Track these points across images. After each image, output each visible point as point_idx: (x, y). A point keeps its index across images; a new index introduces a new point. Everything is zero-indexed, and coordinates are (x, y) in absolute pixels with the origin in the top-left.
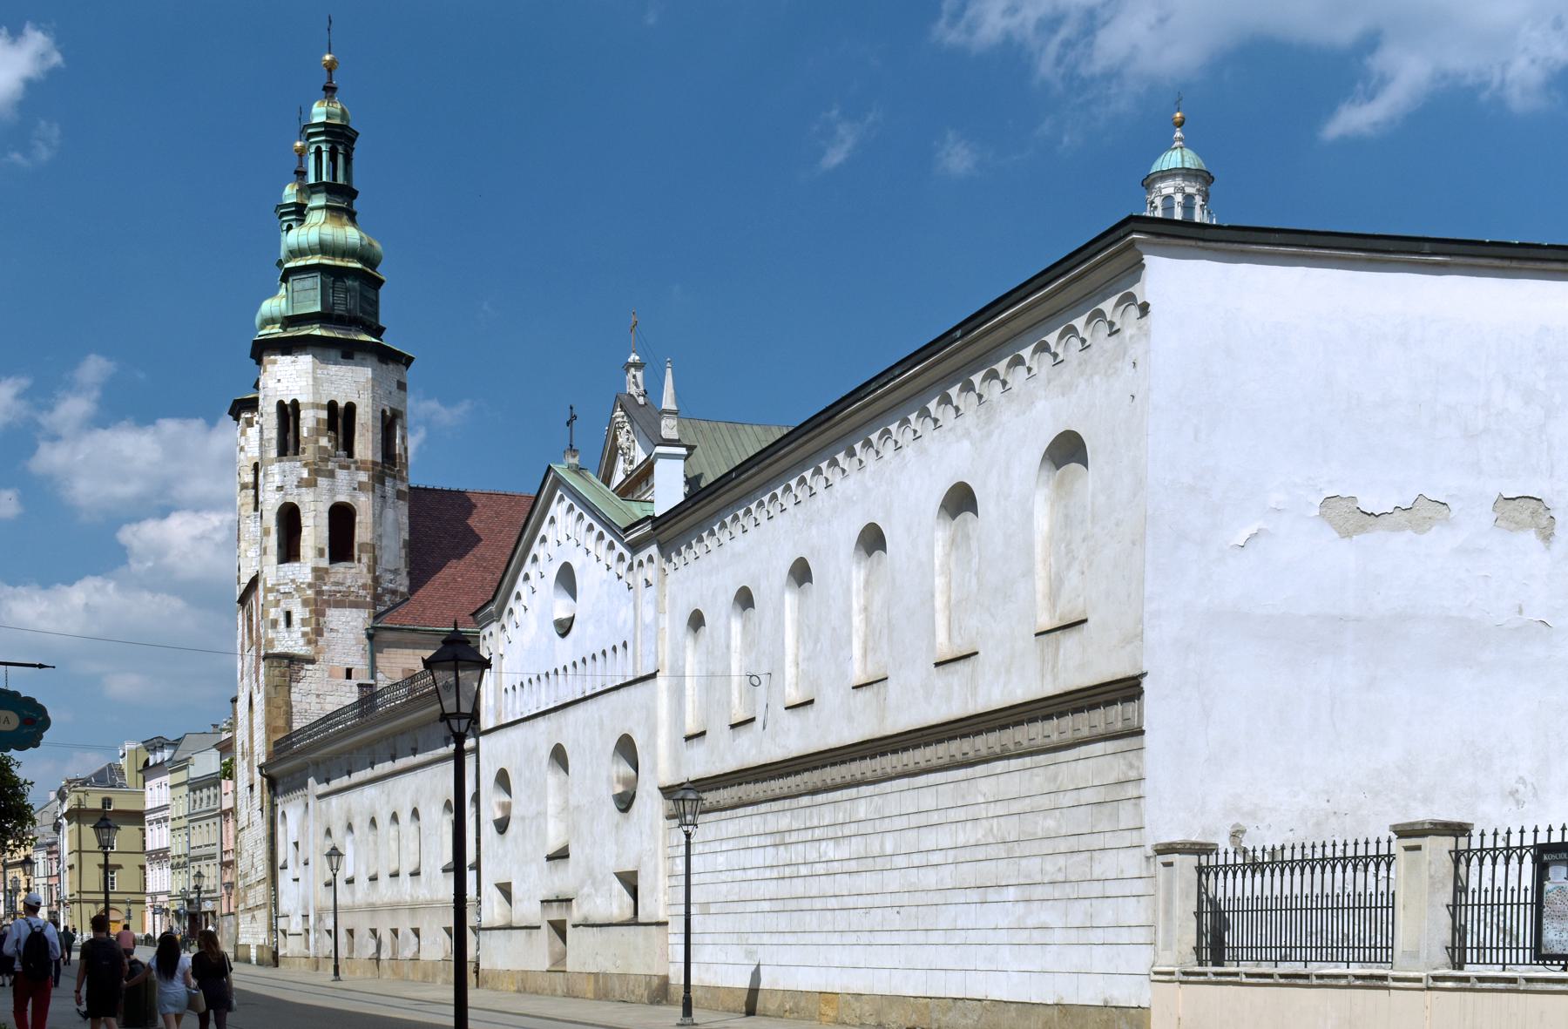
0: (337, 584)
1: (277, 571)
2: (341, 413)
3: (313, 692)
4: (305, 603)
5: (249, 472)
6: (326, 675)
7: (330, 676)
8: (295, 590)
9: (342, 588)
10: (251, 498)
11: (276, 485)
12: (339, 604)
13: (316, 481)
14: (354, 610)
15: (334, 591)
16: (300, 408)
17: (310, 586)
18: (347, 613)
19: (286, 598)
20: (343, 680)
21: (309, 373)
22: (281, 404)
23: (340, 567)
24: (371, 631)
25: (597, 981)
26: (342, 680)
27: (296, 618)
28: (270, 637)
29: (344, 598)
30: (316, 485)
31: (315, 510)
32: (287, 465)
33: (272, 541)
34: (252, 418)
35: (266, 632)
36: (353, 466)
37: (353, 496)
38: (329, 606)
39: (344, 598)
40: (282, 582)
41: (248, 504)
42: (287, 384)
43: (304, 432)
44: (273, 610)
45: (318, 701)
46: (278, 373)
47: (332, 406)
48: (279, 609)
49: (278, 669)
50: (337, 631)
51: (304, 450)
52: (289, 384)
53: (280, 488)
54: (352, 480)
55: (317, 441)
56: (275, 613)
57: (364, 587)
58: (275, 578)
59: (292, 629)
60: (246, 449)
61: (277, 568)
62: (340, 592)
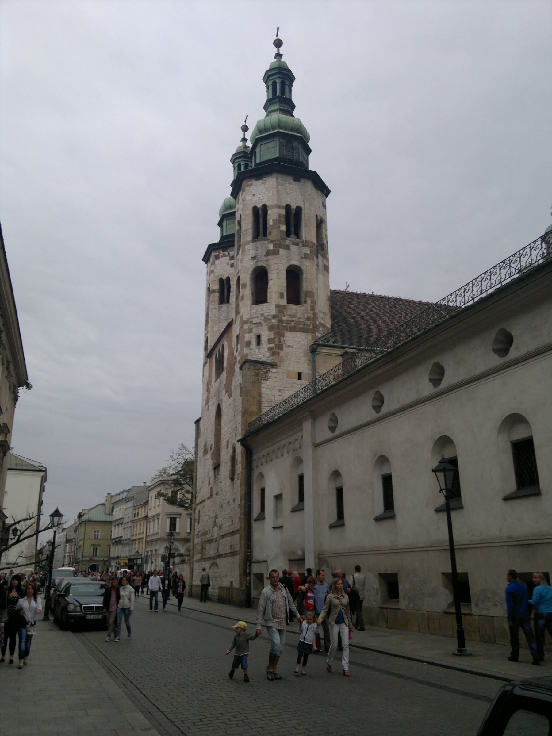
0: (291, 316)
1: (251, 310)
3: (276, 387)
4: (271, 328)
6: (285, 376)
7: (287, 377)
10: (217, 298)
11: (250, 256)
12: (293, 329)
13: (278, 251)
14: (302, 334)
15: (290, 321)
16: (268, 209)
17: (274, 317)
18: (298, 335)
19: (258, 326)
20: (296, 380)
21: (274, 188)
22: (255, 209)
23: (294, 306)
24: (315, 347)
26: (296, 380)
27: (264, 339)
28: (245, 353)
29: (296, 326)
30: (278, 253)
31: (277, 269)
32: (259, 244)
34: (219, 255)
35: (242, 349)
36: (301, 244)
37: (301, 262)
38: (287, 330)
39: (296, 326)
40: (254, 316)
41: (214, 301)
42: (259, 196)
43: (270, 222)
45: (280, 394)
46: (253, 191)
47: (288, 208)
48: (252, 334)
49: (254, 370)
50: (292, 347)
51: (270, 233)
53: (254, 258)
54: (300, 252)
55: (279, 227)
56: (250, 337)
57: (308, 319)
58: (249, 315)
59: (261, 346)
60: (215, 271)
61: (251, 308)
62: (293, 321)
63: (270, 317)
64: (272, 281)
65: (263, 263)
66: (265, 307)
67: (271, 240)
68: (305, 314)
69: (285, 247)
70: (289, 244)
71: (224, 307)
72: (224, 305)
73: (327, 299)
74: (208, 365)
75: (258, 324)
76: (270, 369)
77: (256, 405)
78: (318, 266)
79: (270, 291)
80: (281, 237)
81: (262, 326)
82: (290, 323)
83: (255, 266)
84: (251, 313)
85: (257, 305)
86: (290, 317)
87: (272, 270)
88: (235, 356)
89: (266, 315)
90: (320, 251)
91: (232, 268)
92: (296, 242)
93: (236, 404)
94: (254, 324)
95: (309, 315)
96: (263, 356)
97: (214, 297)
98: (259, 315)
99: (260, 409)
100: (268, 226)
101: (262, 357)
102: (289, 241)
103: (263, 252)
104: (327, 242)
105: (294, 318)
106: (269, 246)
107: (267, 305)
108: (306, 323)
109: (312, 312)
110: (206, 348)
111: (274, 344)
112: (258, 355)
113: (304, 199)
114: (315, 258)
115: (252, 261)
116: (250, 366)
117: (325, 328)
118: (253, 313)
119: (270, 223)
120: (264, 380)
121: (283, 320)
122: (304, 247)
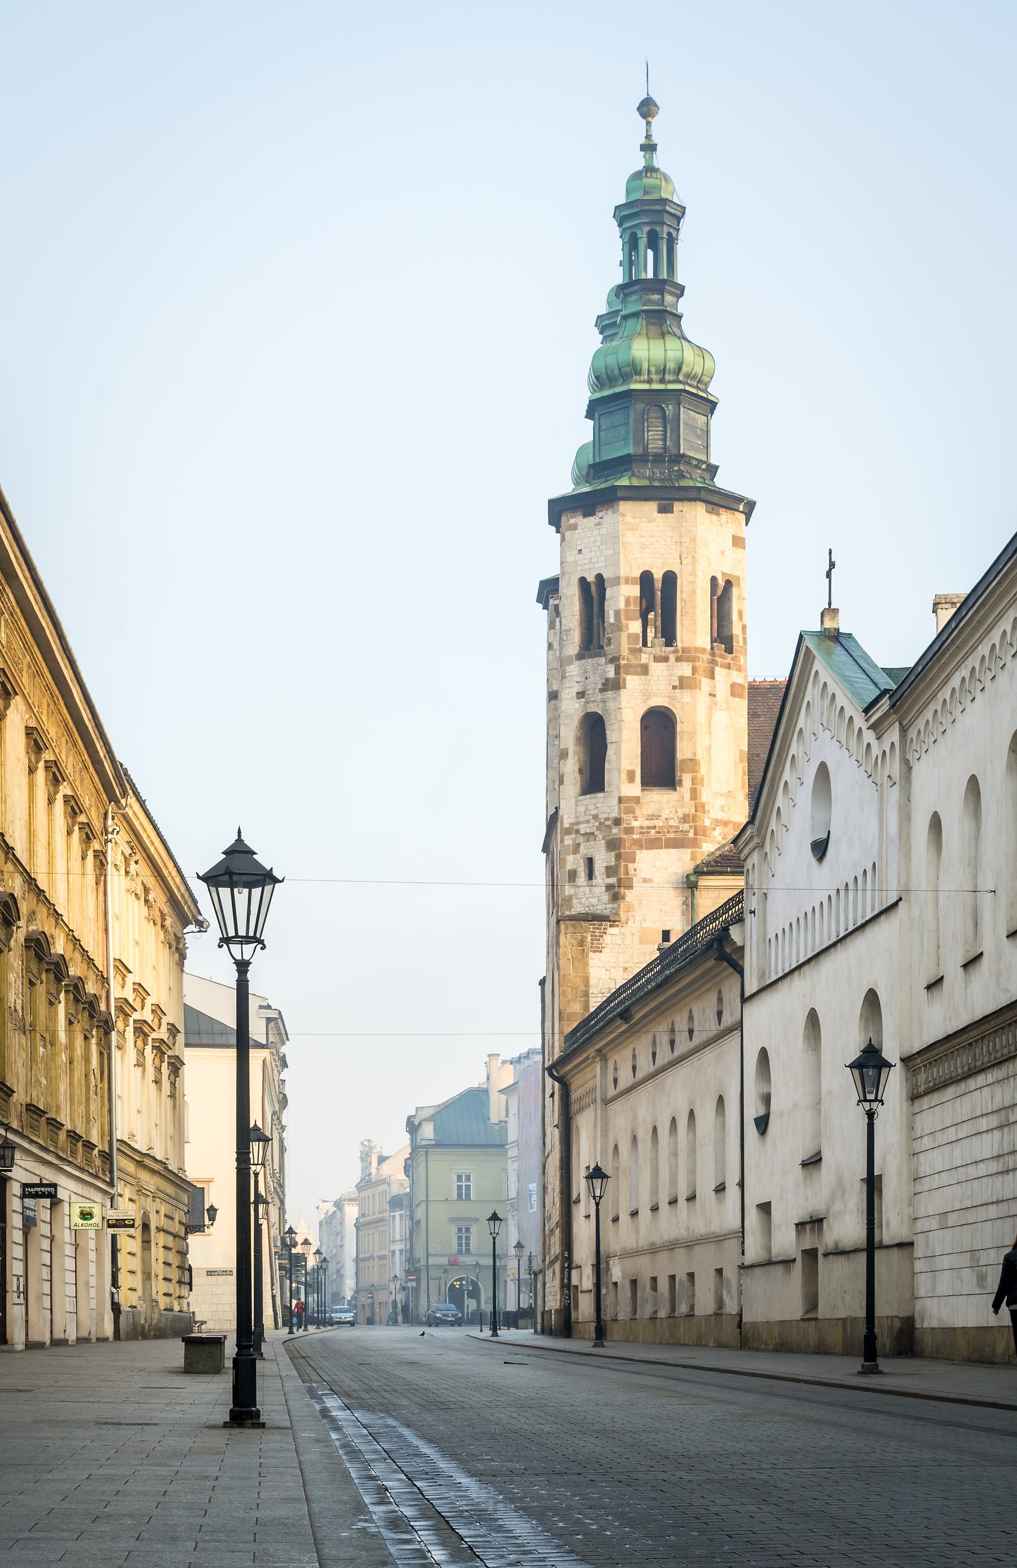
0: (651, 817)
1: (576, 805)
6: (637, 939)
7: (641, 942)
8: (597, 827)
9: (659, 823)
12: (653, 844)
13: (624, 680)
14: (673, 851)
15: (648, 828)
19: (588, 840)
25: (844, 1329)
27: (599, 868)
28: (567, 894)
32: (589, 663)
33: (571, 767)
36: (672, 657)
38: (641, 847)
39: (658, 836)
40: (582, 819)
44: (570, 858)
48: (578, 856)
50: (651, 880)
52: (593, 555)
53: (581, 695)
54: (672, 675)
56: (574, 862)
57: (685, 819)
59: (594, 881)
61: (576, 801)
62: (654, 827)
64: (614, 746)
65: (597, 705)
67: (610, 657)
68: (679, 810)
69: (639, 669)
73: (738, 759)
75: (589, 836)
76: (606, 929)
77: (580, 1001)
78: (713, 695)
79: (609, 767)
80: (630, 649)
81: (595, 840)
82: (648, 832)
83: (582, 712)
84: (576, 812)
85: (587, 796)
87: (612, 722)
90: (719, 660)
92: (664, 655)
94: (582, 835)
95: (687, 811)
96: (599, 900)
98: (591, 817)
102: (647, 656)
103: (595, 682)
104: (744, 627)
106: (606, 670)
107: (605, 797)
108: (681, 829)
109: (693, 803)
111: (615, 879)
112: (590, 899)
113: (681, 552)
114: (705, 682)
115: (578, 701)
116: (567, 928)
117: (731, 825)
118: (581, 812)
120: (594, 952)
121: (633, 827)
122: (679, 664)
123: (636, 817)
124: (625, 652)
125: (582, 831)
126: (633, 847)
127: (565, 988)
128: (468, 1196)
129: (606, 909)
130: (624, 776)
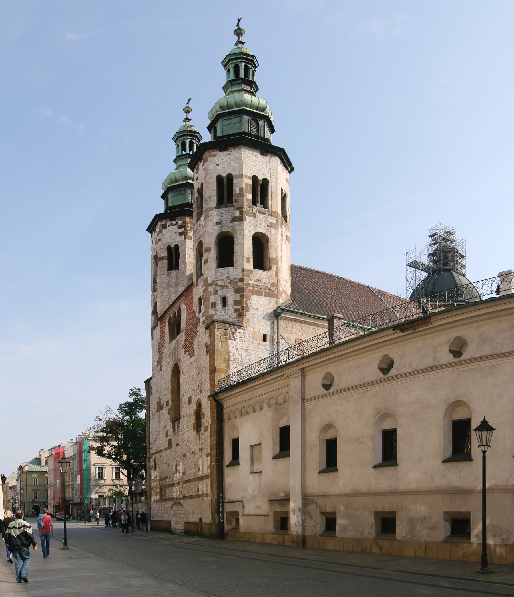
1: (216, 272)
2: (260, 183)
5: (164, 251)
7: (253, 338)
12: (258, 293)
13: (245, 217)
15: (256, 285)
19: (223, 289)
20: (261, 341)
24: (279, 311)
26: (260, 341)
27: (230, 301)
28: (210, 314)
32: (223, 210)
35: (207, 311)
38: (253, 293)
40: (219, 279)
41: (163, 267)
45: (246, 354)
48: (217, 296)
51: (236, 201)
59: (227, 308)
61: (216, 271)
62: (259, 286)
63: (237, 280)
64: (239, 245)
65: (229, 228)
66: (230, 270)
67: (237, 207)
70: (256, 212)
71: (173, 273)
72: (173, 271)
74: (158, 328)
75: (224, 287)
79: (236, 255)
80: (247, 205)
82: (256, 287)
86: (256, 281)
87: (239, 235)
88: (198, 317)
89: (232, 278)
91: (180, 236)
93: (200, 363)
94: (219, 286)
96: (230, 317)
97: (163, 263)
99: (228, 367)
100: (233, 194)
101: (228, 318)
105: (260, 283)
107: (233, 269)
108: (271, 289)
110: (155, 312)
112: (224, 316)
118: (218, 276)
119: (236, 191)
121: (249, 284)
123: (251, 279)
124: (245, 204)
125: (219, 284)
126: (250, 293)
127: (218, 356)
128: (37, 484)
129: (234, 321)
130: (245, 259)
